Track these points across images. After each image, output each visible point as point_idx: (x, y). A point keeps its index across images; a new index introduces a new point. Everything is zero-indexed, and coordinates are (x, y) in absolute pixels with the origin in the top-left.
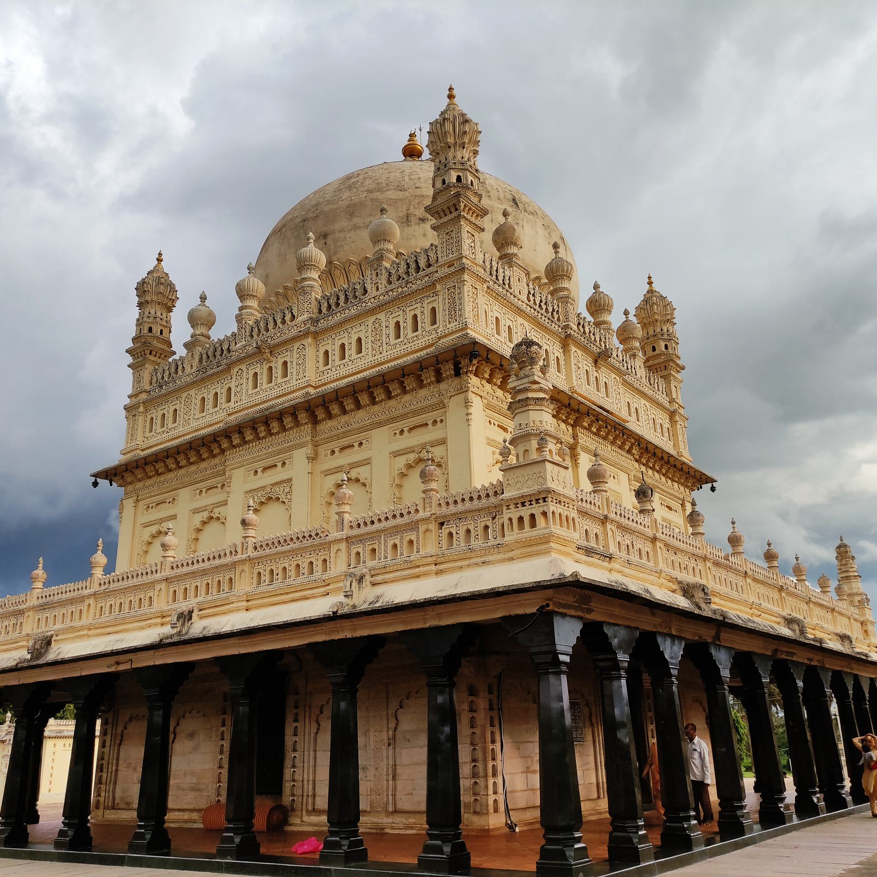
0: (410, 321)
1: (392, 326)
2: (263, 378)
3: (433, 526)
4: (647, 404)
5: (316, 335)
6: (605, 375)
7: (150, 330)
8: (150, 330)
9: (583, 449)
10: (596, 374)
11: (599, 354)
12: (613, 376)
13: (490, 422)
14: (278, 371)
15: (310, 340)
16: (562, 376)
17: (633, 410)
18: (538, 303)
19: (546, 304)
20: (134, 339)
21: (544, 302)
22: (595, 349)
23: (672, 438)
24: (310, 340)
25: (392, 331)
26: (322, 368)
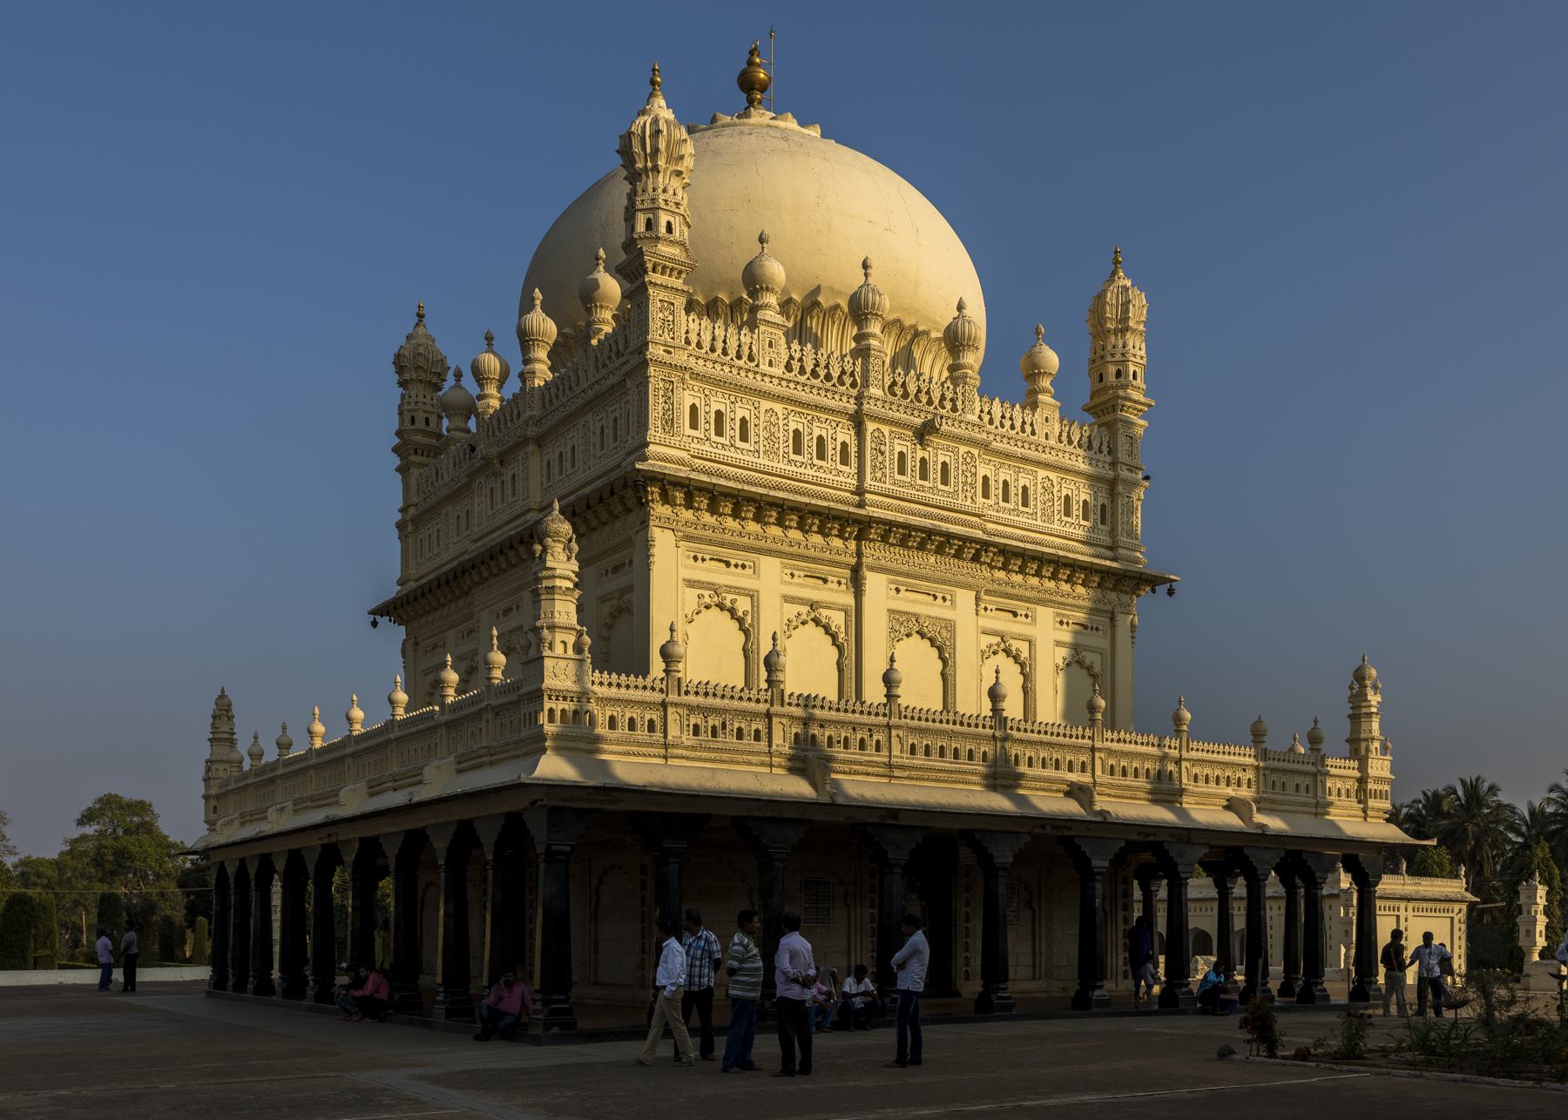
0: (611, 426)
1: (598, 432)
2: (498, 494)
3: (490, 716)
4: (1053, 476)
5: (540, 441)
6: (938, 454)
7: (413, 420)
8: (413, 420)
9: (872, 569)
10: (920, 454)
11: (924, 425)
12: (963, 449)
13: (695, 558)
14: (508, 486)
15: (531, 448)
16: (852, 469)
17: (1012, 491)
18: (808, 370)
19: (827, 367)
20: (398, 434)
21: (823, 364)
22: (919, 421)
23: (1108, 519)
24: (531, 448)
25: (597, 440)
26: (546, 485)
